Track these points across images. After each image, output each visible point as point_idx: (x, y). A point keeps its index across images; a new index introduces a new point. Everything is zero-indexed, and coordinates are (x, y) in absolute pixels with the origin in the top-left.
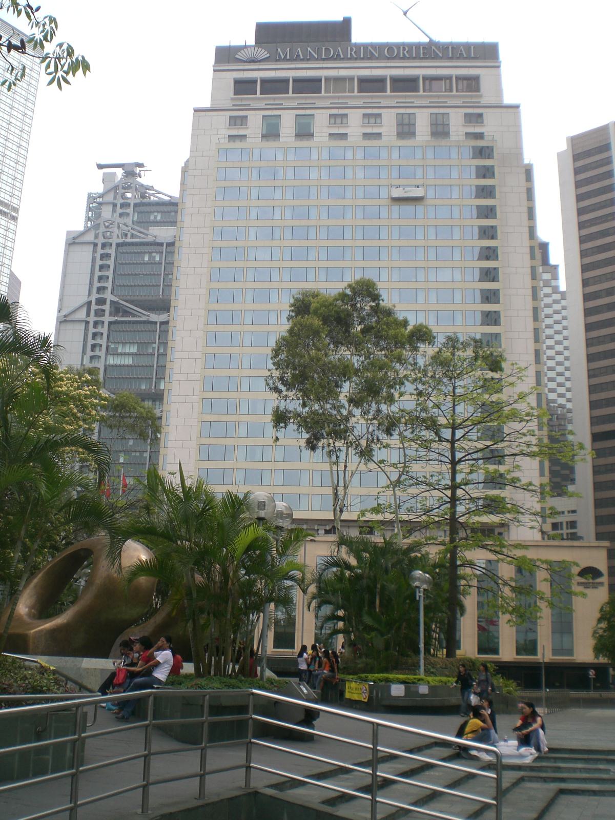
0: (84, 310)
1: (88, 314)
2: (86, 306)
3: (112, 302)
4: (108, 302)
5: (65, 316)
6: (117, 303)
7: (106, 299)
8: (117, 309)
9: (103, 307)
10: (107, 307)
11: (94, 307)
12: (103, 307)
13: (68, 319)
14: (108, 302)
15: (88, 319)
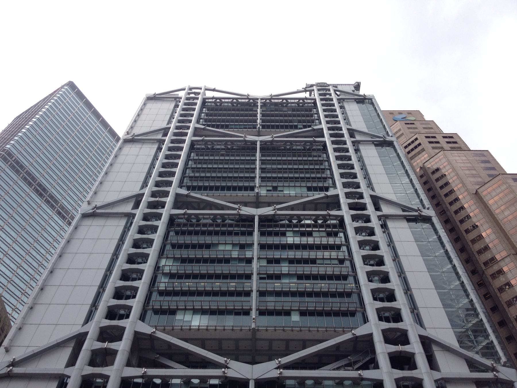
0: (66, 353)
1: (72, 362)
2: (72, 344)
3: (138, 336)
4: (128, 336)
5: (14, 364)
6: (151, 337)
7: (123, 329)
8: (145, 351)
9: (113, 346)
10: (122, 347)
11: (91, 344)
12: (113, 346)
13: (17, 370)
14: (128, 336)
15: (68, 371)
